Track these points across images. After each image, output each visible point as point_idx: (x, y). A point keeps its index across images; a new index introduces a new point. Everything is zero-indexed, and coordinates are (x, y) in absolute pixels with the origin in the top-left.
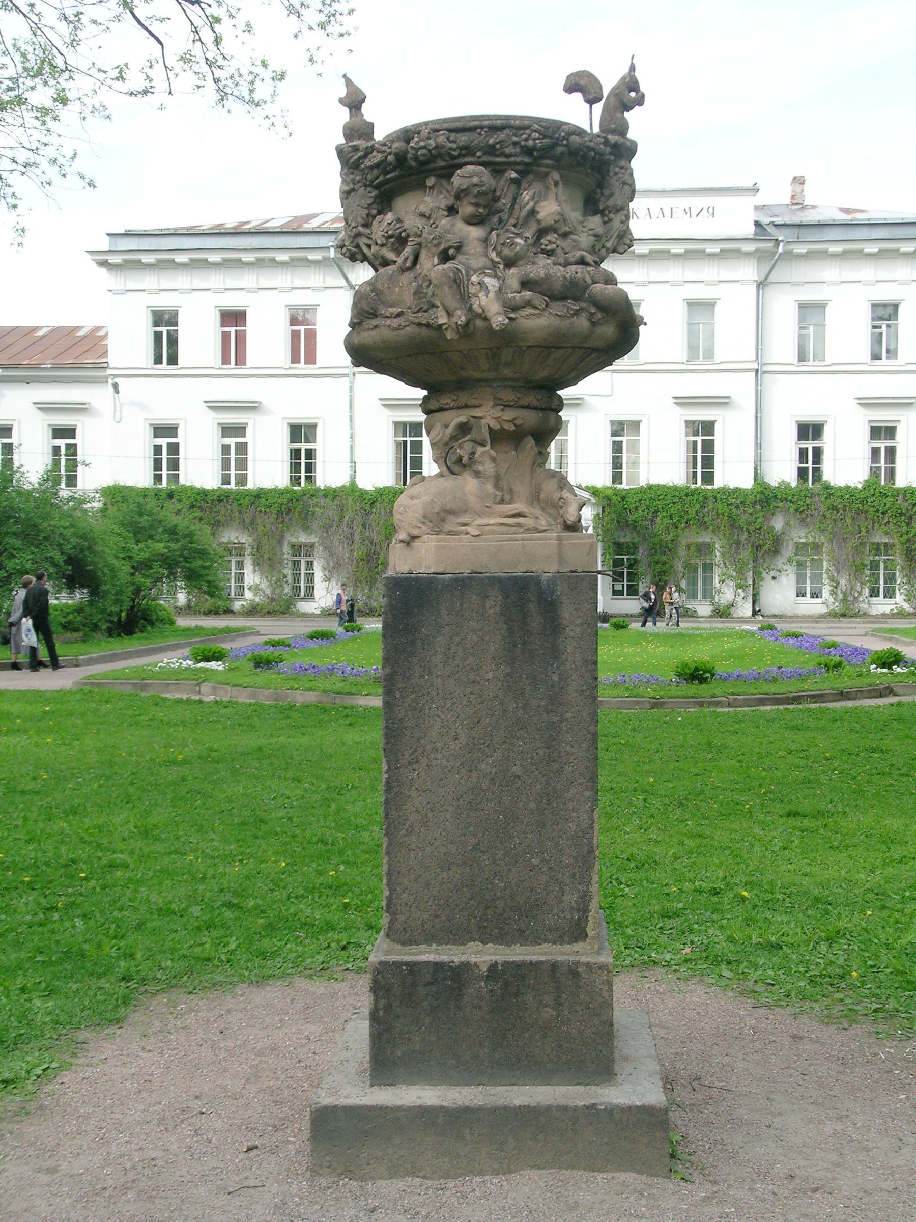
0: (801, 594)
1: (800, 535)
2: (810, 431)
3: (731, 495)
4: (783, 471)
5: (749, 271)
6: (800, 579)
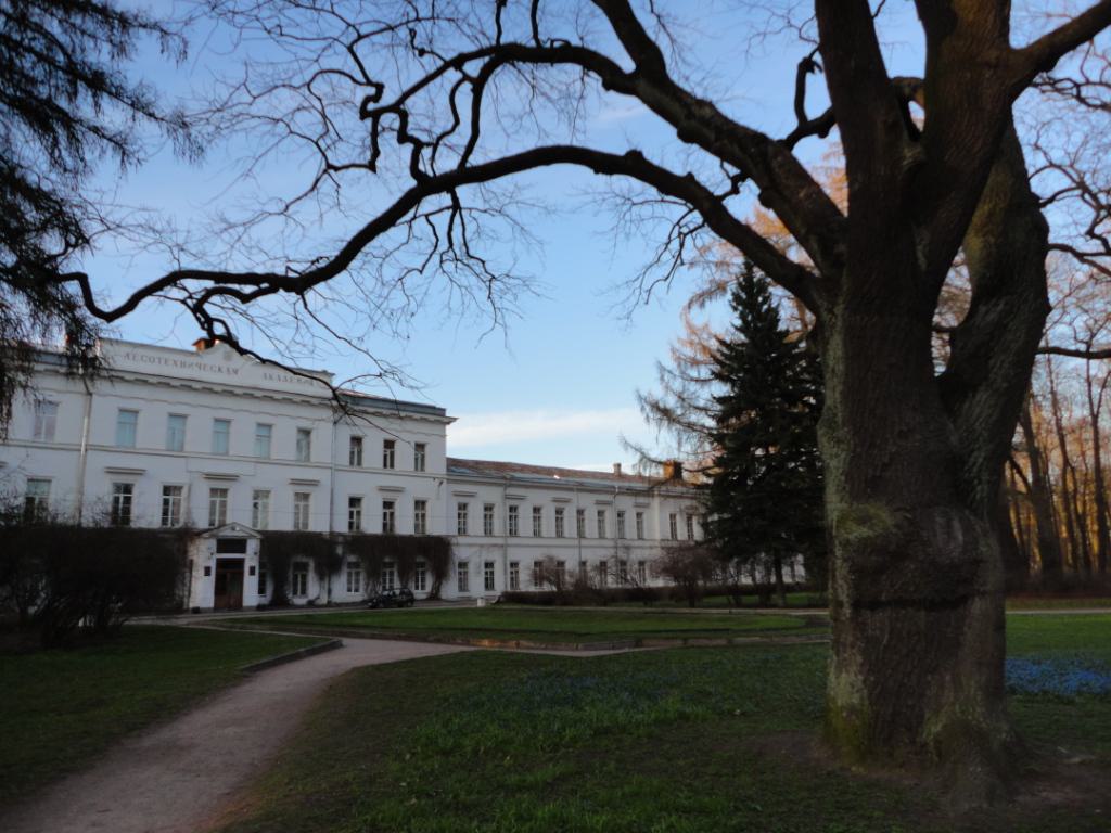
0: (349, 590)
1: (352, 558)
2: (354, 502)
3: (318, 535)
4: (342, 527)
5: (328, 414)
6: (349, 582)
